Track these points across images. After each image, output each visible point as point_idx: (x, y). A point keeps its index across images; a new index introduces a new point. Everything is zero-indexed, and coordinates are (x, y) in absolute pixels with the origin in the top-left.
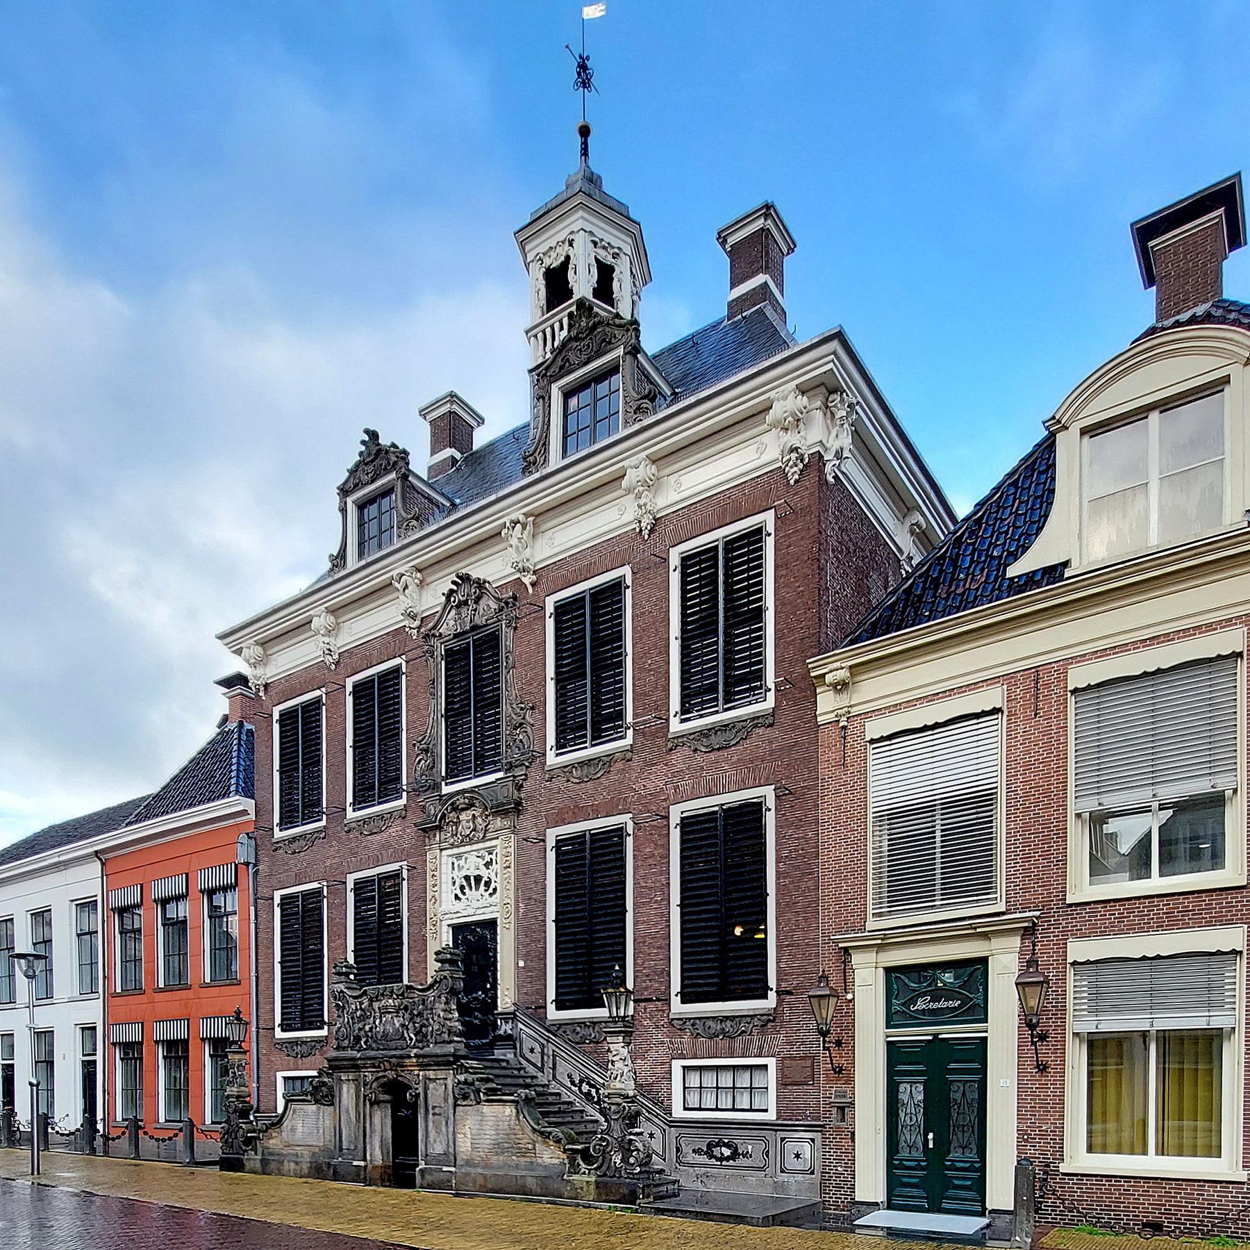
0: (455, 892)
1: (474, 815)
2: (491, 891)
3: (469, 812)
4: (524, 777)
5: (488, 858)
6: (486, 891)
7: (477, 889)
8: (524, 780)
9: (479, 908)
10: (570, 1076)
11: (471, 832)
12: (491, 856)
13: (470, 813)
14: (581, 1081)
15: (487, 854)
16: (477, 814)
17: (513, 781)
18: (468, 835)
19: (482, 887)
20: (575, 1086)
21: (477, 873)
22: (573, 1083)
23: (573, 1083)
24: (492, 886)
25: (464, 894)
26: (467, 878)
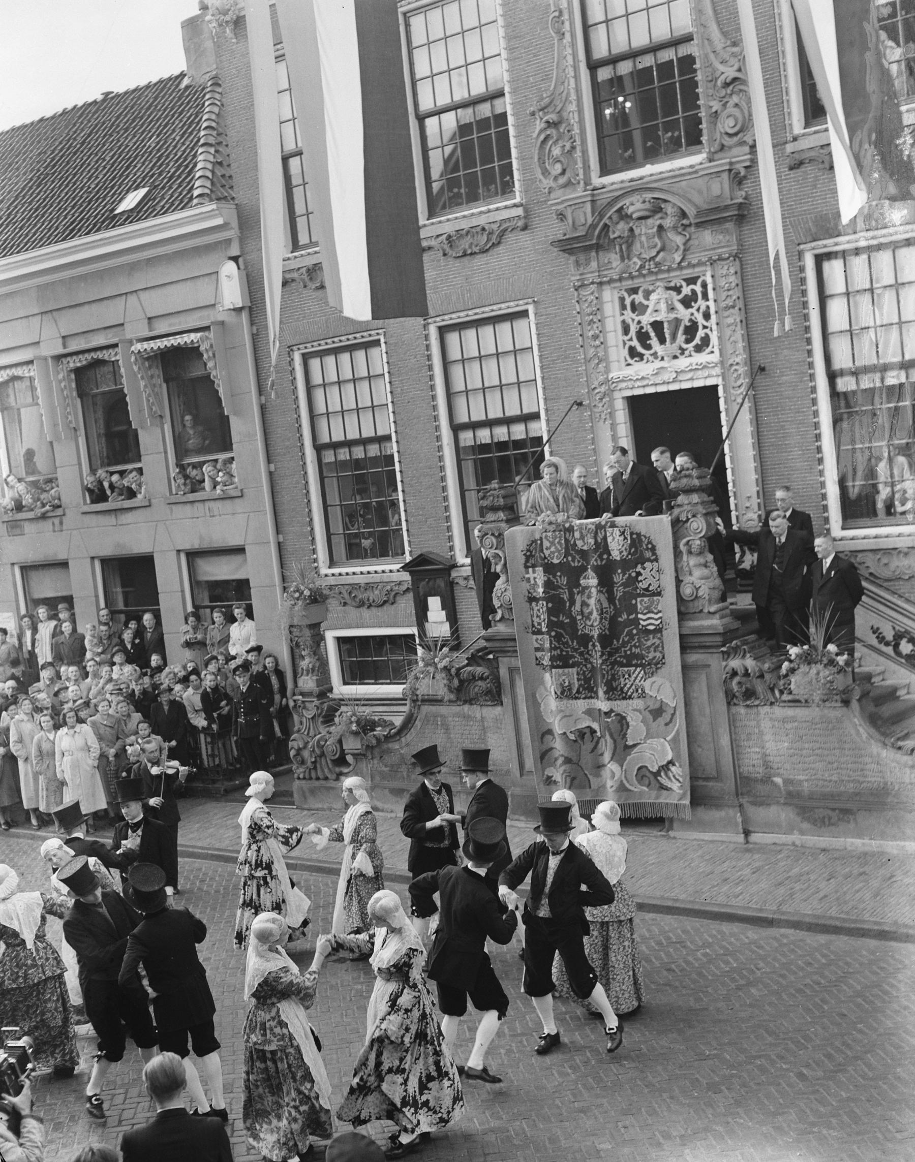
0: (629, 344)
1: (660, 227)
2: (697, 340)
3: (650, 221)
4: (748, 164)
5: (686, 290)
6: (688, 341)
7: (674, 337)
8: (746, 167)
9: (682, 371)
10: (875, 631)
11: (658, 253)
12: (692, 287)
13: (654, 222)
14: (898, 637)
15: (684, 284)
16: (668, 222)
17: (730, 170)
18: (653, 258)
19: (681, 338)
20: (887, 644)
21: (672, 316)
22: (881, 639)
23: (881, 639)
24: (701, 333)
25: (649, 347)
26: (657, 326)
